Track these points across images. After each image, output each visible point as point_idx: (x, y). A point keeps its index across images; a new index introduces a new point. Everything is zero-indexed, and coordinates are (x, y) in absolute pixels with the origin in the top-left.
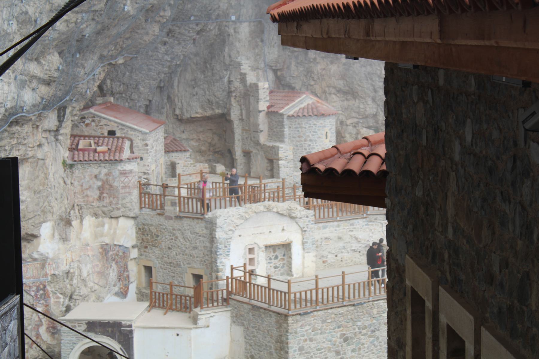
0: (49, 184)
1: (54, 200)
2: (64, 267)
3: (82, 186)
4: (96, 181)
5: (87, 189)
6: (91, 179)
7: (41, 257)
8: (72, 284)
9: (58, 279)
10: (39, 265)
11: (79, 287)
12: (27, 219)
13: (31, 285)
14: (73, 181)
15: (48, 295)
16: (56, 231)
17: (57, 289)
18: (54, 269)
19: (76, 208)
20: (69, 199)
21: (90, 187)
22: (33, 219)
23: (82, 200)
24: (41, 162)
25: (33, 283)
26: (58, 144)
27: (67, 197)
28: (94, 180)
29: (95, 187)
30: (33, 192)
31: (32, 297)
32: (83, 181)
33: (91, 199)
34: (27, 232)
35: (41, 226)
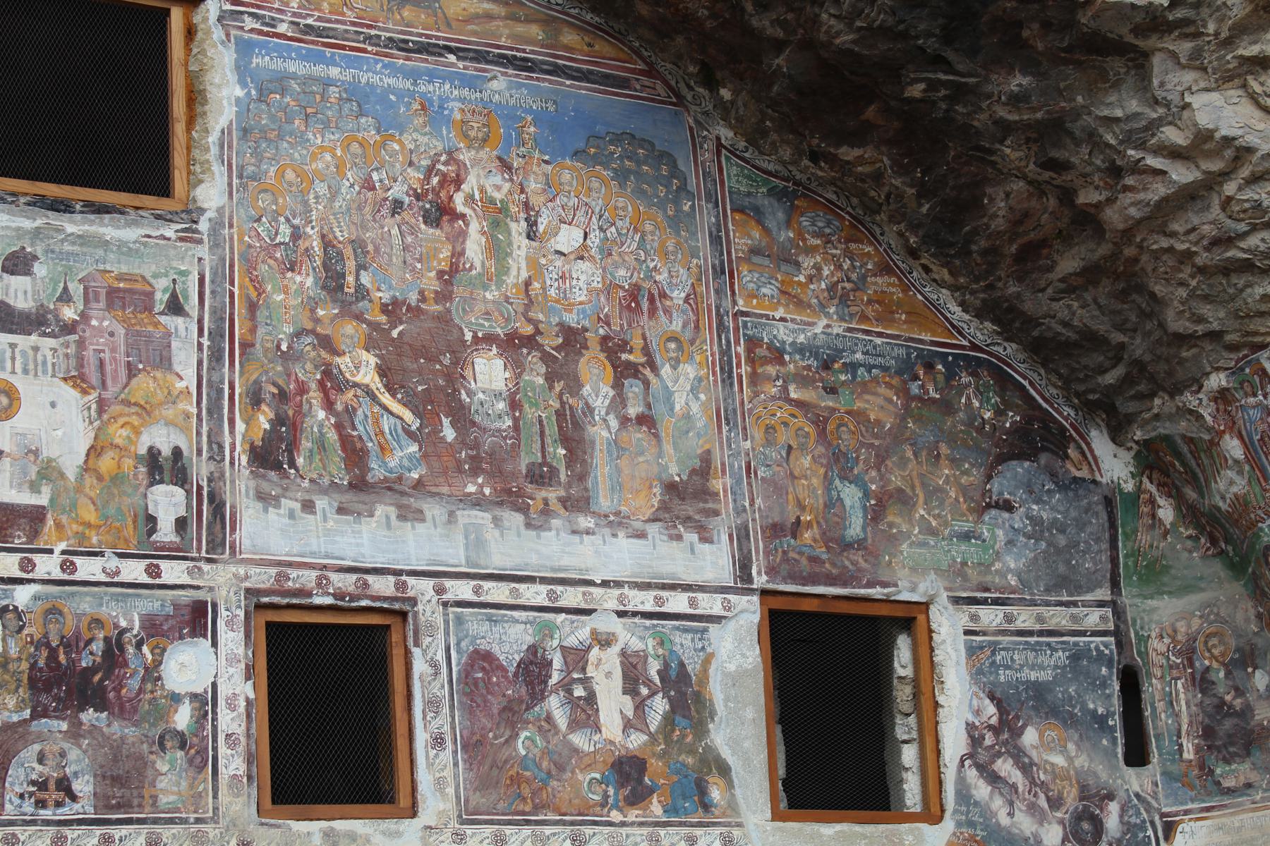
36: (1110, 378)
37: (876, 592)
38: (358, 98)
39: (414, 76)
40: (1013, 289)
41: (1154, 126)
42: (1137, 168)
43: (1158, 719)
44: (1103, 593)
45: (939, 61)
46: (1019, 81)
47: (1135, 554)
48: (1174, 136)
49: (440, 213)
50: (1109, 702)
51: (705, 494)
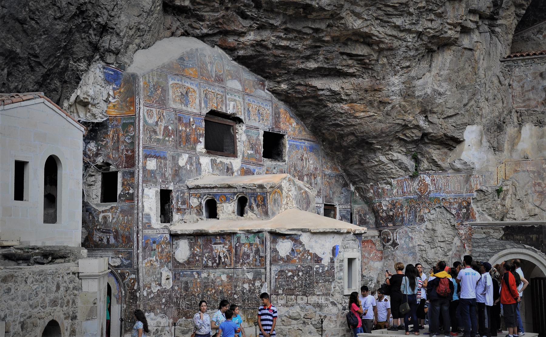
0: (478, 80)
1: (484, 100)
2: (493, 183)
3: (522, 87)
4: (541, 81)
5: (529, 91)
6: (535, 79)
7: (465, 167)
8: (504, 203)
9: (486, 197)
10: (462, 178)
11: (512, 208)
12: (445, 116)
13: (452, 201)
14: (511, 82)
15: (473, 215)
16: (484, 136)
17: (485, 209)
18: (481, 184)
19: (514, 116)
20: (505, 102)
21: (533, 88)
22: (454, 118)
23: (522, 105)
24: (467, 53)
25: (454, 199)
26: (494, 37)
27: (502, 99)
28: (539, 78)
29: (540, 87)
30: (455, 85)
31: (453, 216)
32: (525, 80)
33: (533, 103)
34: (445, 132)
35: (465, 128)
36: (357, 180)
37: (332, 204)
38: (297, 146)
39: (300, 143)
40: (348, 168)
41: (375, 158)
42: (371, 162)
43: (354, 219)
44: (350, 204)
45: (355, 148)
46: (361, 151)
47: (353, 199)
48: (377, 160)
49: (302, 160)
50: (349, 217)
51: (320, 192)
